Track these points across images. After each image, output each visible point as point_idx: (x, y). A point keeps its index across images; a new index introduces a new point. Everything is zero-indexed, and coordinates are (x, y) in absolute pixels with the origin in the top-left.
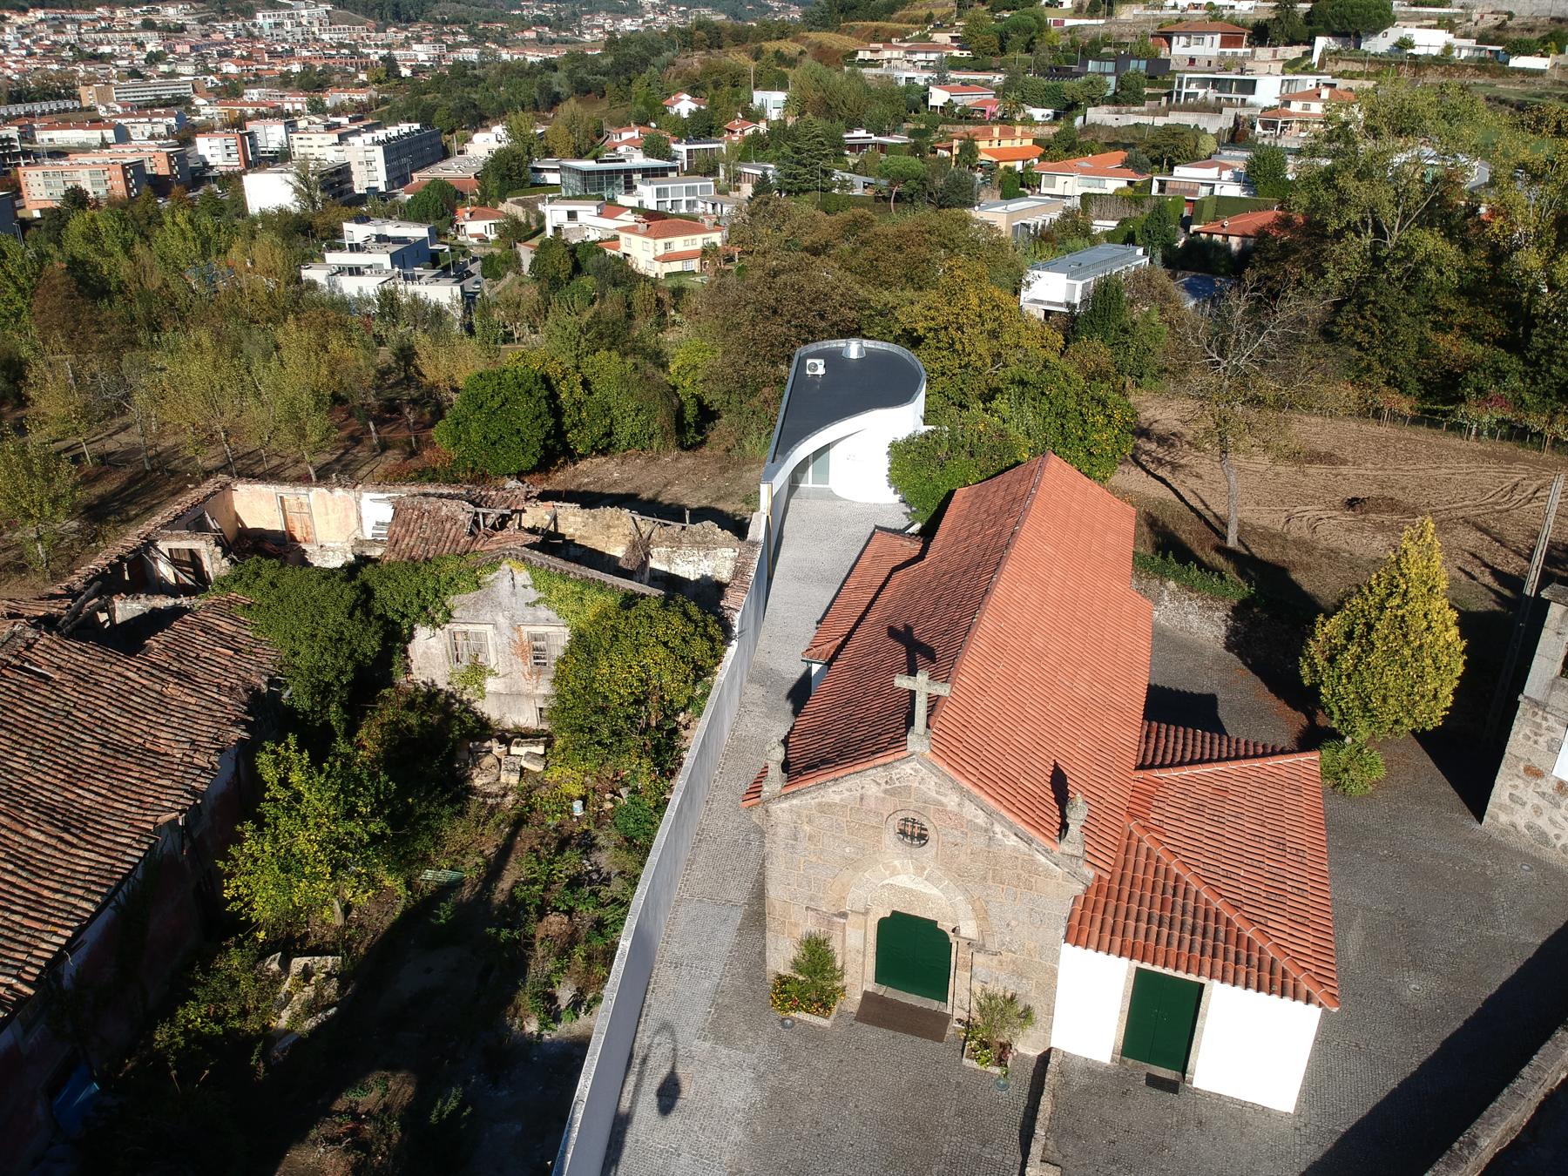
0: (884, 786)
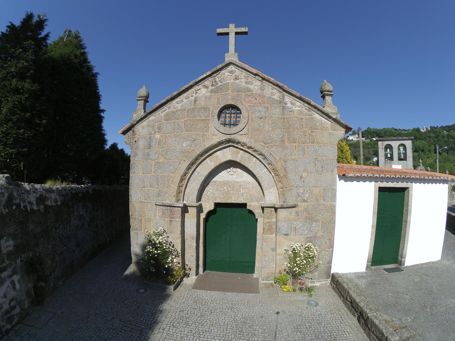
0: (211, 88)
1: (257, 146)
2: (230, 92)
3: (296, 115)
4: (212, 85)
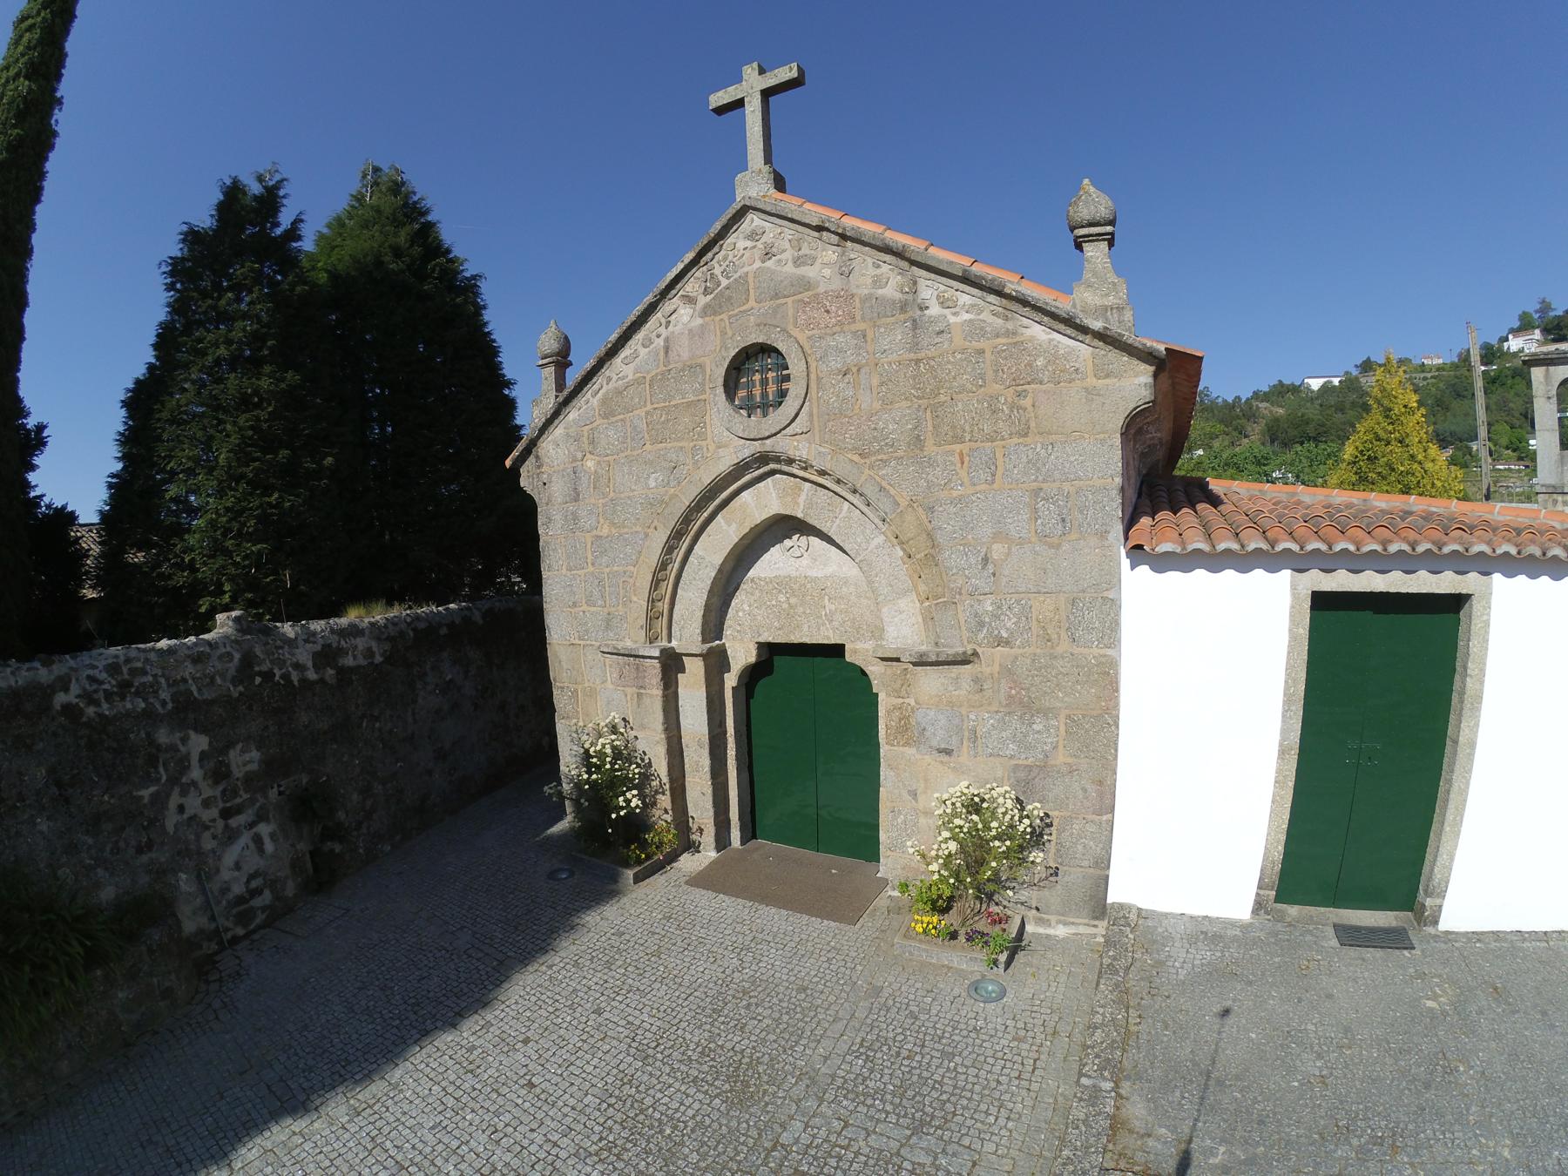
0: (703, 300)
1: (840, 467)
2: (752, 303)
3: (958, 341)
4: (706, 292)
